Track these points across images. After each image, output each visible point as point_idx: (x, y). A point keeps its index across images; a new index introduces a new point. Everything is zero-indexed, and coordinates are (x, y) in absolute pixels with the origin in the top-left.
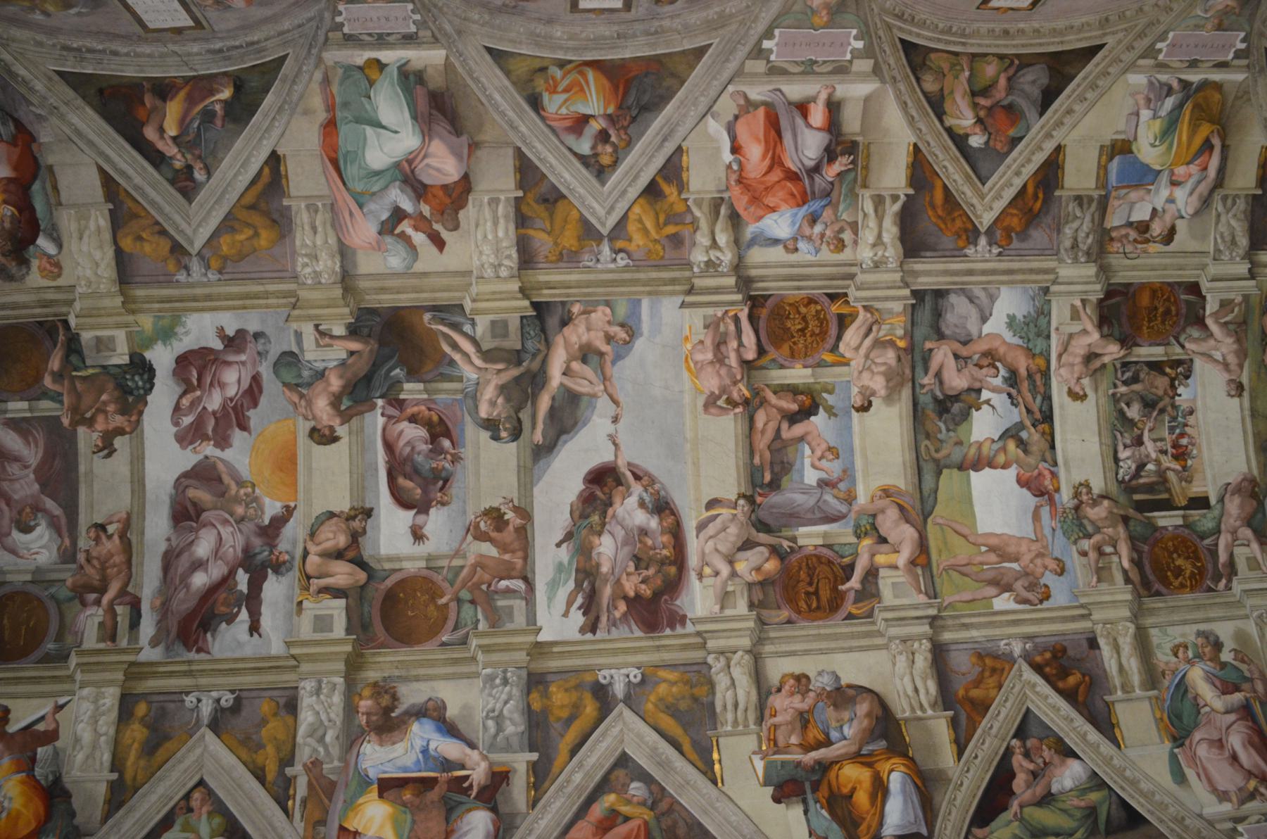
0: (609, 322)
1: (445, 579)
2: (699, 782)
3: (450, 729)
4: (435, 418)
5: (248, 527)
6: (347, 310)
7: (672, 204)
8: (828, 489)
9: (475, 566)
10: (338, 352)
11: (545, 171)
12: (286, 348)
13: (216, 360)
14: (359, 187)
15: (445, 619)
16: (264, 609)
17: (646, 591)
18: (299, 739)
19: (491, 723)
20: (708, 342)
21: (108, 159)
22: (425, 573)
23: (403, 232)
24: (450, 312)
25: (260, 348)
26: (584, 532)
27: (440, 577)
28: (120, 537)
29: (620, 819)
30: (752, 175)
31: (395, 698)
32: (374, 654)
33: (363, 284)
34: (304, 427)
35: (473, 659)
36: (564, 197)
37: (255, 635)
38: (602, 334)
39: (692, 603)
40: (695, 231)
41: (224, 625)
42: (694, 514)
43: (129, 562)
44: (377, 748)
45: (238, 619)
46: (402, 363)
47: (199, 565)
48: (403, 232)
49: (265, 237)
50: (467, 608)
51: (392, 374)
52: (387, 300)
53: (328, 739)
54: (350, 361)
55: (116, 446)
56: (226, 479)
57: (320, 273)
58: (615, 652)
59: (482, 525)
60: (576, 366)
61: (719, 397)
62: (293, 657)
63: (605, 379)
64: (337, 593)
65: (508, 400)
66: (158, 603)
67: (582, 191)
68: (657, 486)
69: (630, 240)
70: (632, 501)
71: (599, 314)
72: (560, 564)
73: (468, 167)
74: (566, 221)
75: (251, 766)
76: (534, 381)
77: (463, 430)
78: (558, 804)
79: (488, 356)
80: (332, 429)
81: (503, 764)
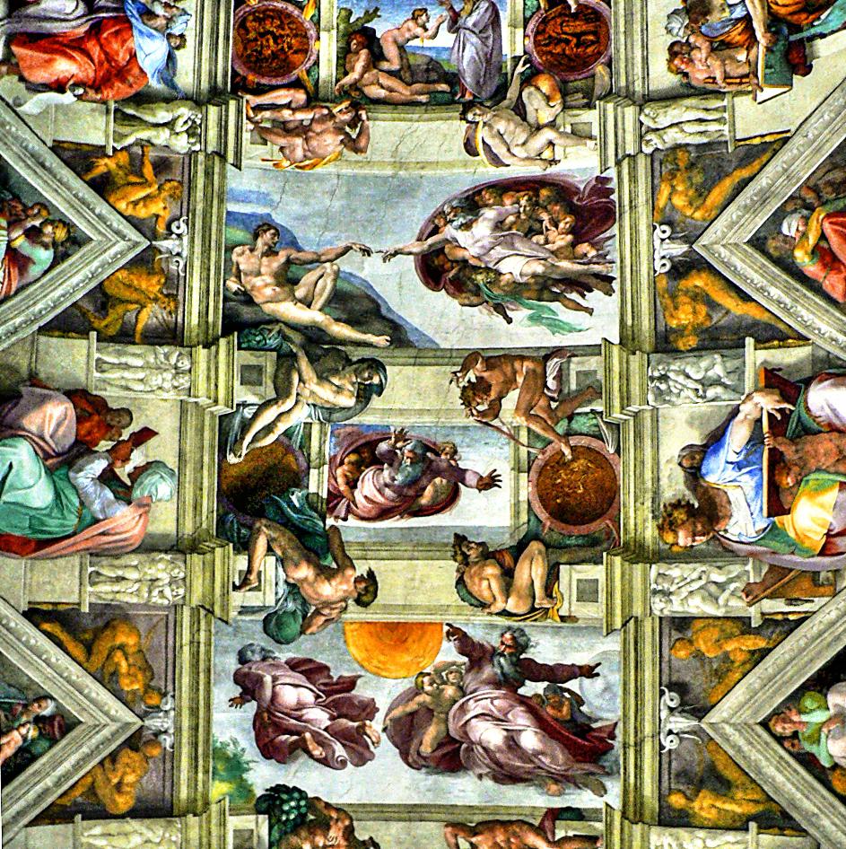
0: (252, 250)
1: (543, 452)
2: (785, 158)
3: (715, 439)
4: (353, 457)
5: (470, 682)
6: (218, 551)
7: (120, 167)
8: (461, 22)
9: (529, 417)
10: (267, 565)
11: (68, 304)
12: (259, 627)
13: (269, 711)
14: (73, 520)
16: (568, 662)
17: (567, 222)
18: (720, 613)
19: (711, 393)
20: (282, 141)
21: (21, 814)
23: (129, 475)
24: (227, 434)
25: (257, 657)
26: (497, 292)
28: (475, 834)
29: (824, 244)
30: (91, 74)
31: (677, 505)
32: (625, 530)
33: (188, 528)
34: (354, 613)
35: (636, 415)
36: (101, 284)
37: (596, 671)
38: (264, 259)
40: (153, 145)
41: (584, 709)
42: (481, 169)
43: (505, 824)
44: (733, 521)
45: (578, 692)
46: (284, 491)
47: (512, 742)
48: (129, 475)
49: (125, 638)
50: (575, 426)
51: (298, 505)
52: (209, 503)
53: (721, 578)
54: (279, 552)
55: (366, 838)
56: (412, 706)
57: (172, 577)
58: (635, 254)
59: (480, 408)
60: (300, 292)
61: (347, 134)
62: (624, 625)
63: (317, 260)
64: (552, 576)
65: (336, 372)
66: (554, 788)
67: (96, 263)
68: (447, 209)
69: (157, 216)
70: (463, 237)
71: (241, 259)
72: (531, 318)
73: (58, 390)
74: (130, 286)
75: (748, 666)
76: (314, 338)
77: (369, 426)
78: (804, 312)
79: (282, 392)
80: (358, 580)
81: (756, 375)
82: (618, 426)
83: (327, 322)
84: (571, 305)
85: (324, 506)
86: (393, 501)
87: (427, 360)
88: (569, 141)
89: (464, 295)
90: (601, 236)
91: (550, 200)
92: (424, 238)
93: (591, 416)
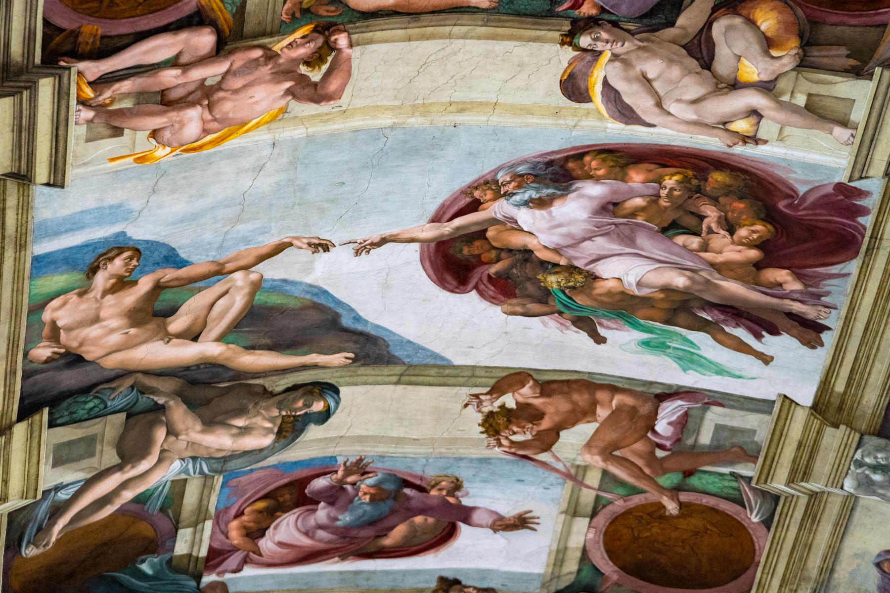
1: (624, 498)
15: (714, 510)
22: (602, 520)
27: (620, 503)
35: (814, 496)
39: (814, 167)
42: (590, 123)
51: (149, 571)
60: (177, 324)
61: (303, 80)
65: (241, 412)
68: (502, 177)
70: (526, 218)
77: (296, 464)
82: (776, 498)
83: (229, 354)
84: (729, 342)
85: (201, 566)
86: (329, 542)
87: (421, 379)
88: (795, 119)
89: (515, 301)
90: (821, 270)
91: (728, 191)
92: (448, 216)
93: (729, 478)
